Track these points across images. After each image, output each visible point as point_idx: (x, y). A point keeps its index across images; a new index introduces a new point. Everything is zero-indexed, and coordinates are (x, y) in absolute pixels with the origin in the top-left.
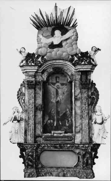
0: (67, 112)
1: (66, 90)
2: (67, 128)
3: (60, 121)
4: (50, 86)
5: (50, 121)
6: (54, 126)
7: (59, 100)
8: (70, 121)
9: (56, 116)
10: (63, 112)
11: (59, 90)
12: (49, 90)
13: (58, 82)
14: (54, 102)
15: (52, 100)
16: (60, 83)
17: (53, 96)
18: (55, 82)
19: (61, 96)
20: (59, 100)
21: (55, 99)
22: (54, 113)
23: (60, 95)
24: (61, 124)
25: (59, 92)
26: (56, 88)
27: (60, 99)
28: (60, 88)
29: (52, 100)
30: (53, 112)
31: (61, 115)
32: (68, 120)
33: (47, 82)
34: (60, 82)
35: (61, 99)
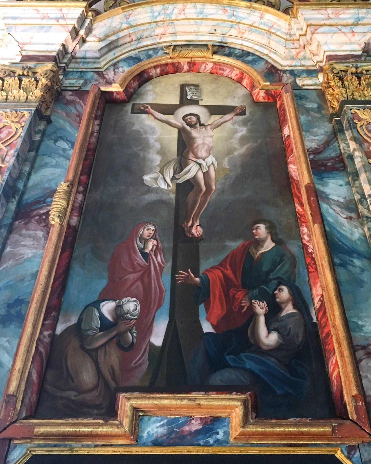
0: (259, 243)
1: (239, 135)
2: (272, 361)
3: (202, 308)
4: (144, 116)
5: (119, 307)
6: (152, 345)
7: (201, 176)
8: (289, 309)
9: (174, 272)
10: (224, 247)
11: (194, 133)
12: (138, 132)
13: (195, 102)
14: (163, 186)
15: (147, 178)
16: (206, 106)
17: (157, 159)
18: (176, 101)
19: (211, 159)
20: (201, 176)
21: (169, 173)
22: (157, 250)
23: (202, 153)
24: (207, 328)
25: (199, 141)
26: (180, 123)
27: (206, 175)
28: (201, 125)
29: (147, 178)
30: (151, 245)
31: (204, 266)
32: (274, 296)
33: (124, 102)
34: (201, 103)
35: (213, 174)
